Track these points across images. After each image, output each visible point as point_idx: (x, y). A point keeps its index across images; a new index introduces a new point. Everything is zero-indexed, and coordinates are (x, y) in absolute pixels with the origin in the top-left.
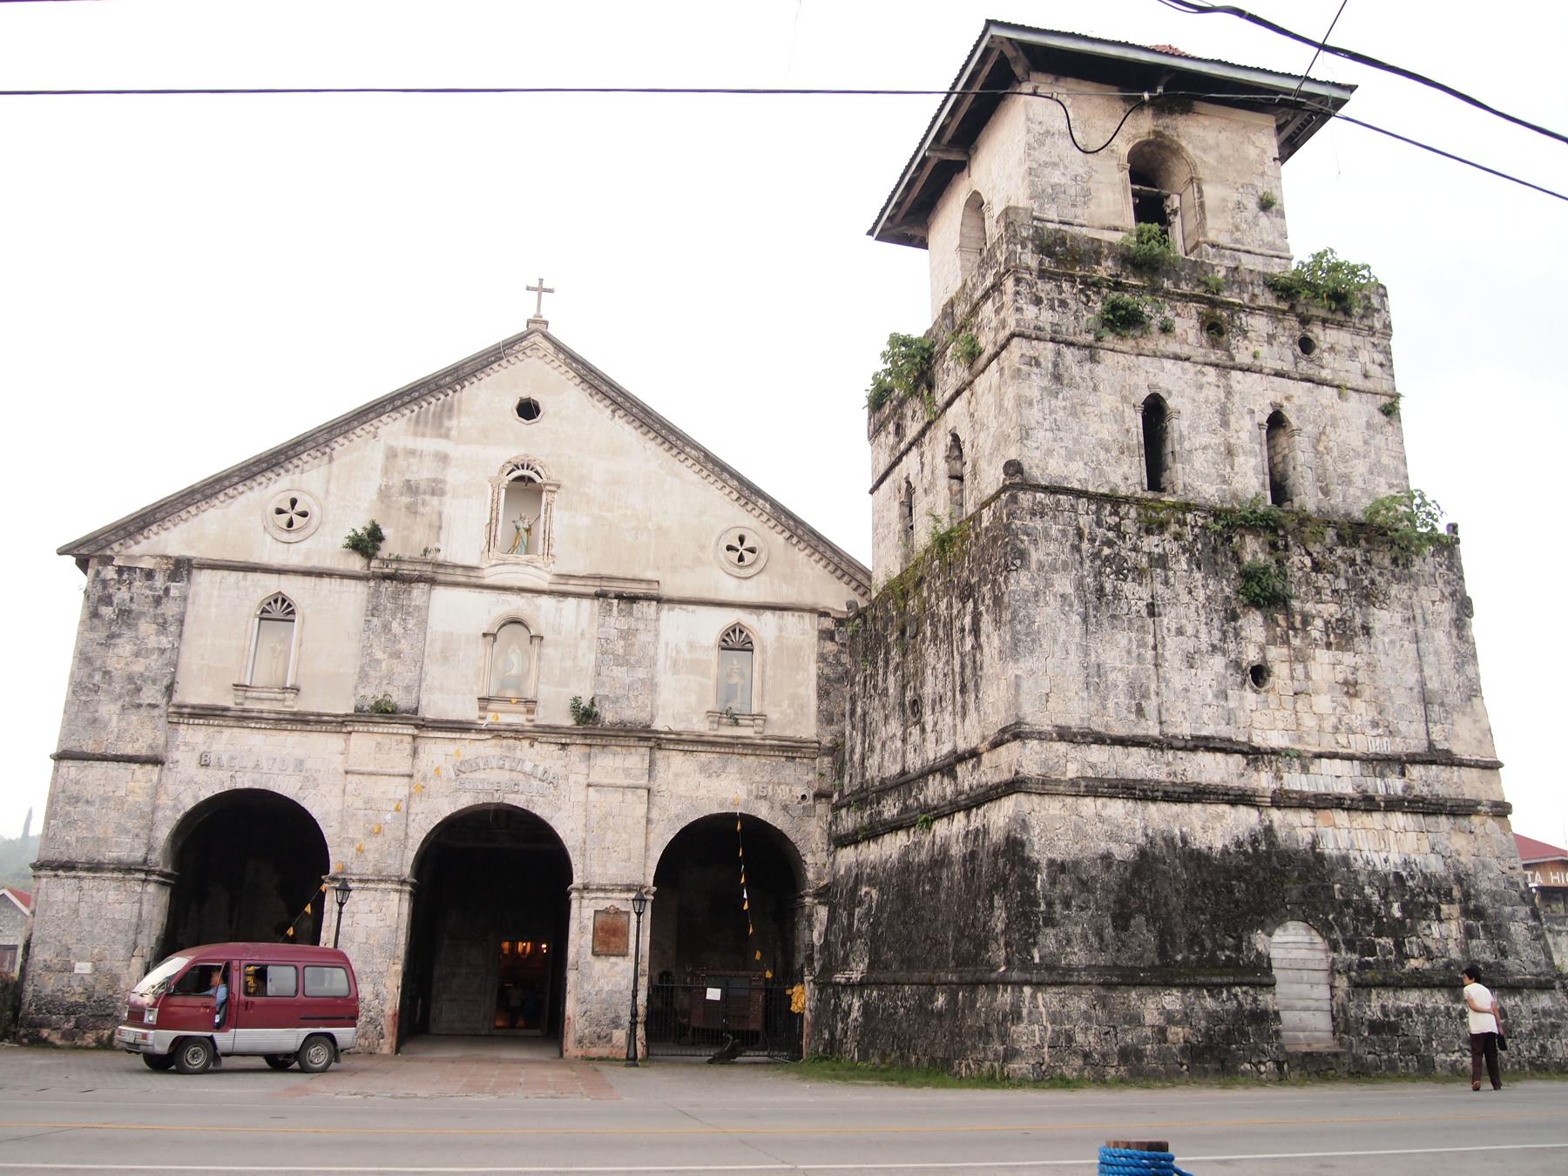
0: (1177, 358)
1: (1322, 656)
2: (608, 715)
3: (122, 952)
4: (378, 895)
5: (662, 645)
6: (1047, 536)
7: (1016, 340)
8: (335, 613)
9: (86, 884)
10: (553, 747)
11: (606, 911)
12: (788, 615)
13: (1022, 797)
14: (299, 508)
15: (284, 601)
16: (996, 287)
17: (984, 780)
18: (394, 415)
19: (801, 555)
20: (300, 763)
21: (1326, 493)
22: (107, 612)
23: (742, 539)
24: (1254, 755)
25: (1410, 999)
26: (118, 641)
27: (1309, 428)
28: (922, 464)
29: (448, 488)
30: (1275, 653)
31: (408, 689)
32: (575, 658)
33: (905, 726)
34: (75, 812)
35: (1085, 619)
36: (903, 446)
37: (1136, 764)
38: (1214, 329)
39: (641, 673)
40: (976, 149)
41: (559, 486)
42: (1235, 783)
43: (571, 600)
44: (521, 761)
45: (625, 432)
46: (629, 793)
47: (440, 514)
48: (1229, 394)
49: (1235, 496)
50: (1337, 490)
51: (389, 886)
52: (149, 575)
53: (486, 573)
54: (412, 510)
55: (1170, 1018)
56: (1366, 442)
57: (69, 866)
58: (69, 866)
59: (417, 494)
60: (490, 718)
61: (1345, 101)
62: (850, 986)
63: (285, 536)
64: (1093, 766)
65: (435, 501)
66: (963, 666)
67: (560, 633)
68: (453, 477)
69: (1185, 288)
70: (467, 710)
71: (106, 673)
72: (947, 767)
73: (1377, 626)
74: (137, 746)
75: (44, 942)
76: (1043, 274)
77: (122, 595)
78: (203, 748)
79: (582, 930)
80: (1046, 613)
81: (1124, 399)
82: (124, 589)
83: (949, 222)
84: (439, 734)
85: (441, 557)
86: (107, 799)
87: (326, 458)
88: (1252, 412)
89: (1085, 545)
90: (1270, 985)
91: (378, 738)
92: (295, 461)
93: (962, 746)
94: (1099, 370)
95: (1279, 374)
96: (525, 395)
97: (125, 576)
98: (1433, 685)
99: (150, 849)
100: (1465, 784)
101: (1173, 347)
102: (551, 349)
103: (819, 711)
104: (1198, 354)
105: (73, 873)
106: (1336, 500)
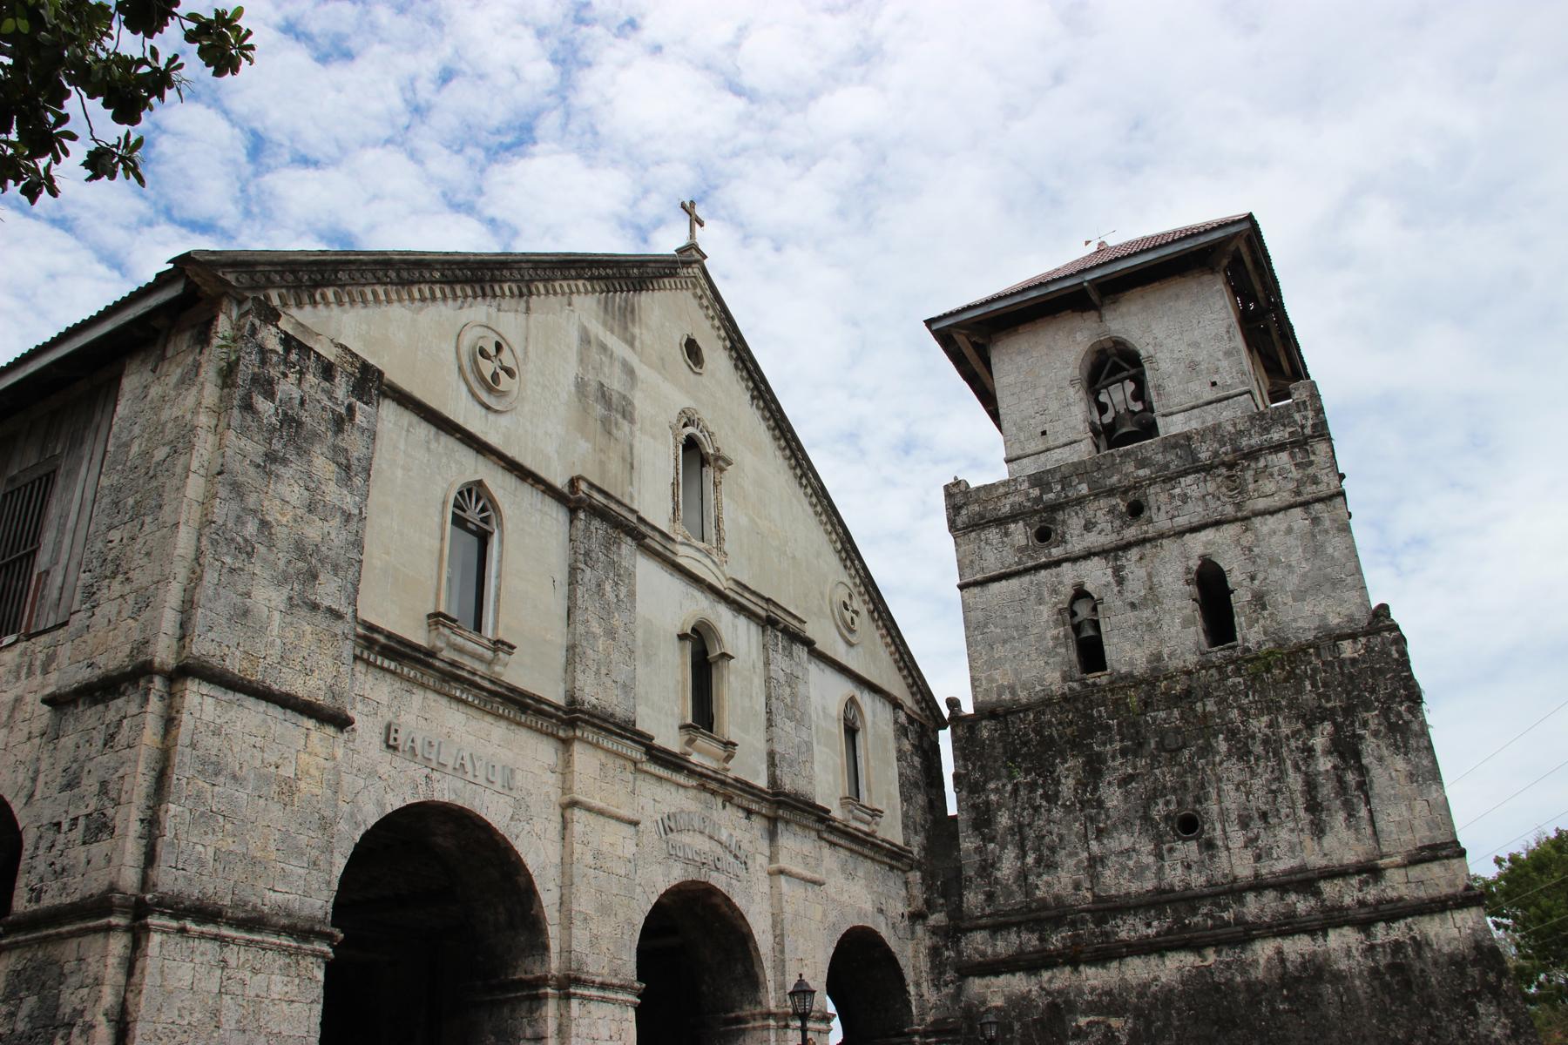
8: (532, 538)
9: (232, 955)
10: (741, 814)
12: (877, 697)
17: (1394, 895)
22: (263, 405)
26: (282, 470)
28: (1120, 581)
33: (1158, 840)
34: (218, 794)
36: (1056, 552)
39: (805, 736)
43: (742, 621)
46: (809, 887)
47: (631, 447)
52: (328, 371)
57: (206, 913)
59: (607, 408)
63: (485, 397)
65: (625, 425)
66: (1311, 786)
68: (642, 404)
71: (264, 524)
72: (1305, 881)
74: (313, 682)
77: (287, 387)
78: (389, 717)
82: (292, 378)
86: (265, 779)
91: (601, 755)
93: (1315, 860)
97: (293, 357)
103: (905, 815)
105: (210, 929)
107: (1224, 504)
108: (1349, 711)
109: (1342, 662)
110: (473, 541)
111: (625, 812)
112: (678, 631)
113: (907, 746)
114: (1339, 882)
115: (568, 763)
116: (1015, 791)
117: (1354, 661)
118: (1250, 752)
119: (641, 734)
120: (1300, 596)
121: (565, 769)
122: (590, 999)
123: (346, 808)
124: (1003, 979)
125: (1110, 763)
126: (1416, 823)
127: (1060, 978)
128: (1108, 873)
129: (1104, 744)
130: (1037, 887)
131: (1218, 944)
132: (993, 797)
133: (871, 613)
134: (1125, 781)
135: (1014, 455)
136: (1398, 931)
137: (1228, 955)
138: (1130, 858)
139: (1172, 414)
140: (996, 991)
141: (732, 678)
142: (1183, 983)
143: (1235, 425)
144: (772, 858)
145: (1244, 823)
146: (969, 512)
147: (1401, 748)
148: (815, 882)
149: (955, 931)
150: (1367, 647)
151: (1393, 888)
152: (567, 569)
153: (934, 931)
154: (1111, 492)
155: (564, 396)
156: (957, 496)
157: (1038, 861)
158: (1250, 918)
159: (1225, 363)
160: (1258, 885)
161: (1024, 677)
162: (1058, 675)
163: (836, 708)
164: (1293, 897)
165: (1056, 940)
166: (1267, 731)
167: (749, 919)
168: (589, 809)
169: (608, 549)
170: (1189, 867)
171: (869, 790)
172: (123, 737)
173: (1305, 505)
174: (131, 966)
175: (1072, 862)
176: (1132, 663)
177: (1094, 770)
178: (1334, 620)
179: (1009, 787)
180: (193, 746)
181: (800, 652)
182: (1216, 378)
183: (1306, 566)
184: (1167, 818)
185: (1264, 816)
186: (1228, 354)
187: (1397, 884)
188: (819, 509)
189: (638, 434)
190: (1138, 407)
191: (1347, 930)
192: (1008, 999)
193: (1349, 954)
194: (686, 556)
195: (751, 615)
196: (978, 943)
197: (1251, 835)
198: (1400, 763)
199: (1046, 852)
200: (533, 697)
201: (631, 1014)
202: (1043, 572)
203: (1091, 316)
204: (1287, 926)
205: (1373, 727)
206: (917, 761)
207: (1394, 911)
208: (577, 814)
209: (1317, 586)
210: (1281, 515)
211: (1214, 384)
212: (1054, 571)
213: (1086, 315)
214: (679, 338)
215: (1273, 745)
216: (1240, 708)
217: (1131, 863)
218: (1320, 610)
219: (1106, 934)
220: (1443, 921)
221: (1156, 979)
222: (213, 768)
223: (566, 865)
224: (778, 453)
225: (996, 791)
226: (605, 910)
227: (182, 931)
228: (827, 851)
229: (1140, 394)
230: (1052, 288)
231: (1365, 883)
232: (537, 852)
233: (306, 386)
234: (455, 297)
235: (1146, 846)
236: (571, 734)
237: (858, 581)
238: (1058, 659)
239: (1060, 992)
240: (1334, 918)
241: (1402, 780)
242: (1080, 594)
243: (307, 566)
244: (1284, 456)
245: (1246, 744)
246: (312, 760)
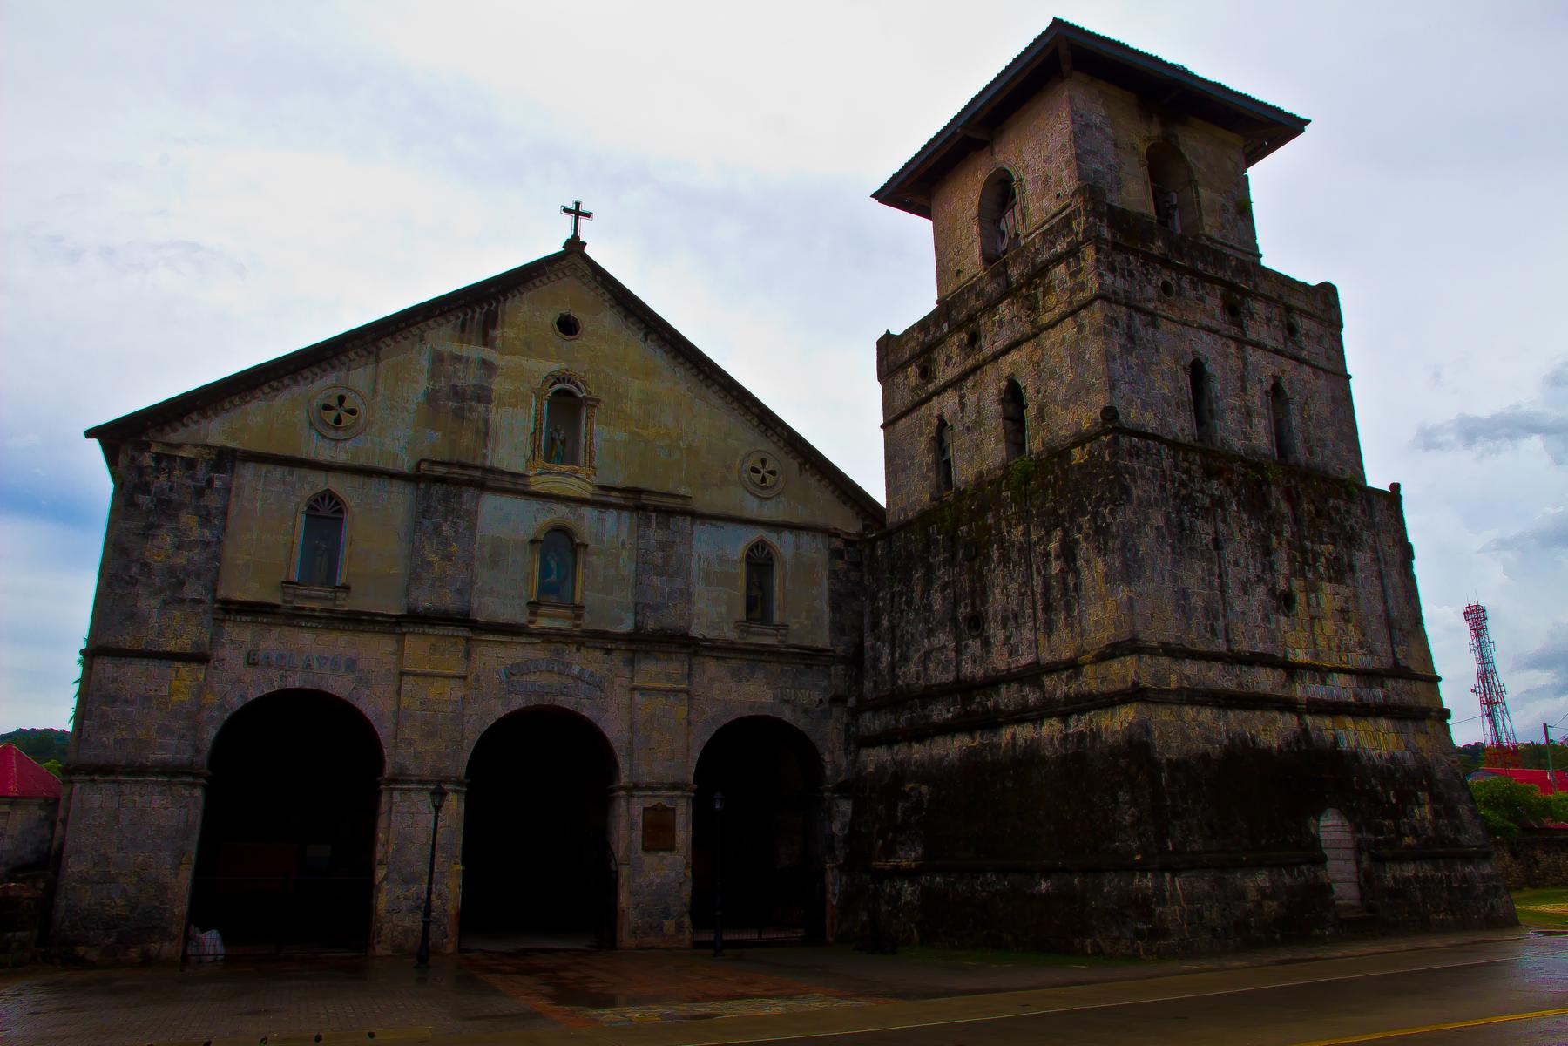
0: (1210, 330)
1: (1327, 587)
5: (695, 556)
6: (1143, 476)
10: (598, 652)
11: (654, 808)
14: (348, 405)
15: (331, 499)
16: (1073, 252)
17: (1085, 689)
18: (441, 320)
20: (352, 665)
21: (1311, 453)
22: (144, 500)
23: (764, 462)
24: (1292, 670)
25: (1409, 870)
27: (1297, 398)
28: (963, 406)
30: (1297, 583)
31: (460, 592)
33: (958, 639)
35: (1173, 551)
36: (930, 388)
37: (1217, 677)
38: (1233, 310)
41: (598, 401)
42: (1280, 693)
44: (569, 665)
45: (658, 358)
47: (487, 421)
48: (1244, 359)
49: (1254, 451)
50: (1317, 450)
52: (190, 464)
54: (459, 415)
55: (1261, 891)
56: (1332, 413)
57: (107, 770)
58: (107, 770)
60: (543, 623)
62: (898, 873)
63: (332, 434)
64: (1188, 678)
65: (481, 408)
66: (1047, 587)
67: (602, 542)
68: (498, 385)
69: (1211, 272)
70: (514, 613)
71: (145, 565)
72: (1034, 674)
73: (1357, 563)
76: (1115, 246)
78: (250, 647)
80: (1146, 543)
81: (1177, 362)
83: (966, 196)
84: (491, 637)
85: (489, 463)
87: (373, 358)
88: (1260, 381)
89: (1168, 486)
90: (1321, 860)
91: (434, 641)
92: (343, 359)
93: (1046, 657)
94: (1158, 335)
95: (1276, 351)
96: (565, 312)
97: (164, 464)
98: (1395, 614)
99: (198, 750)
101: (1206, 321)
102: (589, 271)
104: (1223, 328)
106: (1317, 460)
108: (1072, 516)
112: (531, 533)
114: (1054, 676)
117: (1080, 466)
120: (1065, 408)
121: (400, 653)
122: (410, 790)
124: (874, 751)
127: (901, 751)
136: (1078, 724)
140: (875, 757)
141: (594, 559)
146: (894, 356)
147: (1102, 551)
150: (1090, 453)
156: (887, 344)
157: (901, 655)
160: (1009, 677)
170: (974, 661)
177: (928, 581)
178: (1085, 426)
181: (684, 523)
187: (1091, 681)
191: (1054, 721)
194: (538, 483)
204: (1022, 715)
205: (1085, 531)
208: (405, 678)
214: (550, 318)
215: (1026, 550)
216: (1007, 519)
220: (1113, 715)
225: (883, 599)
227: (93, 781)
232: (374, 704)
242: (942, 424)
243: (177, 577)
244: (1062, 267)
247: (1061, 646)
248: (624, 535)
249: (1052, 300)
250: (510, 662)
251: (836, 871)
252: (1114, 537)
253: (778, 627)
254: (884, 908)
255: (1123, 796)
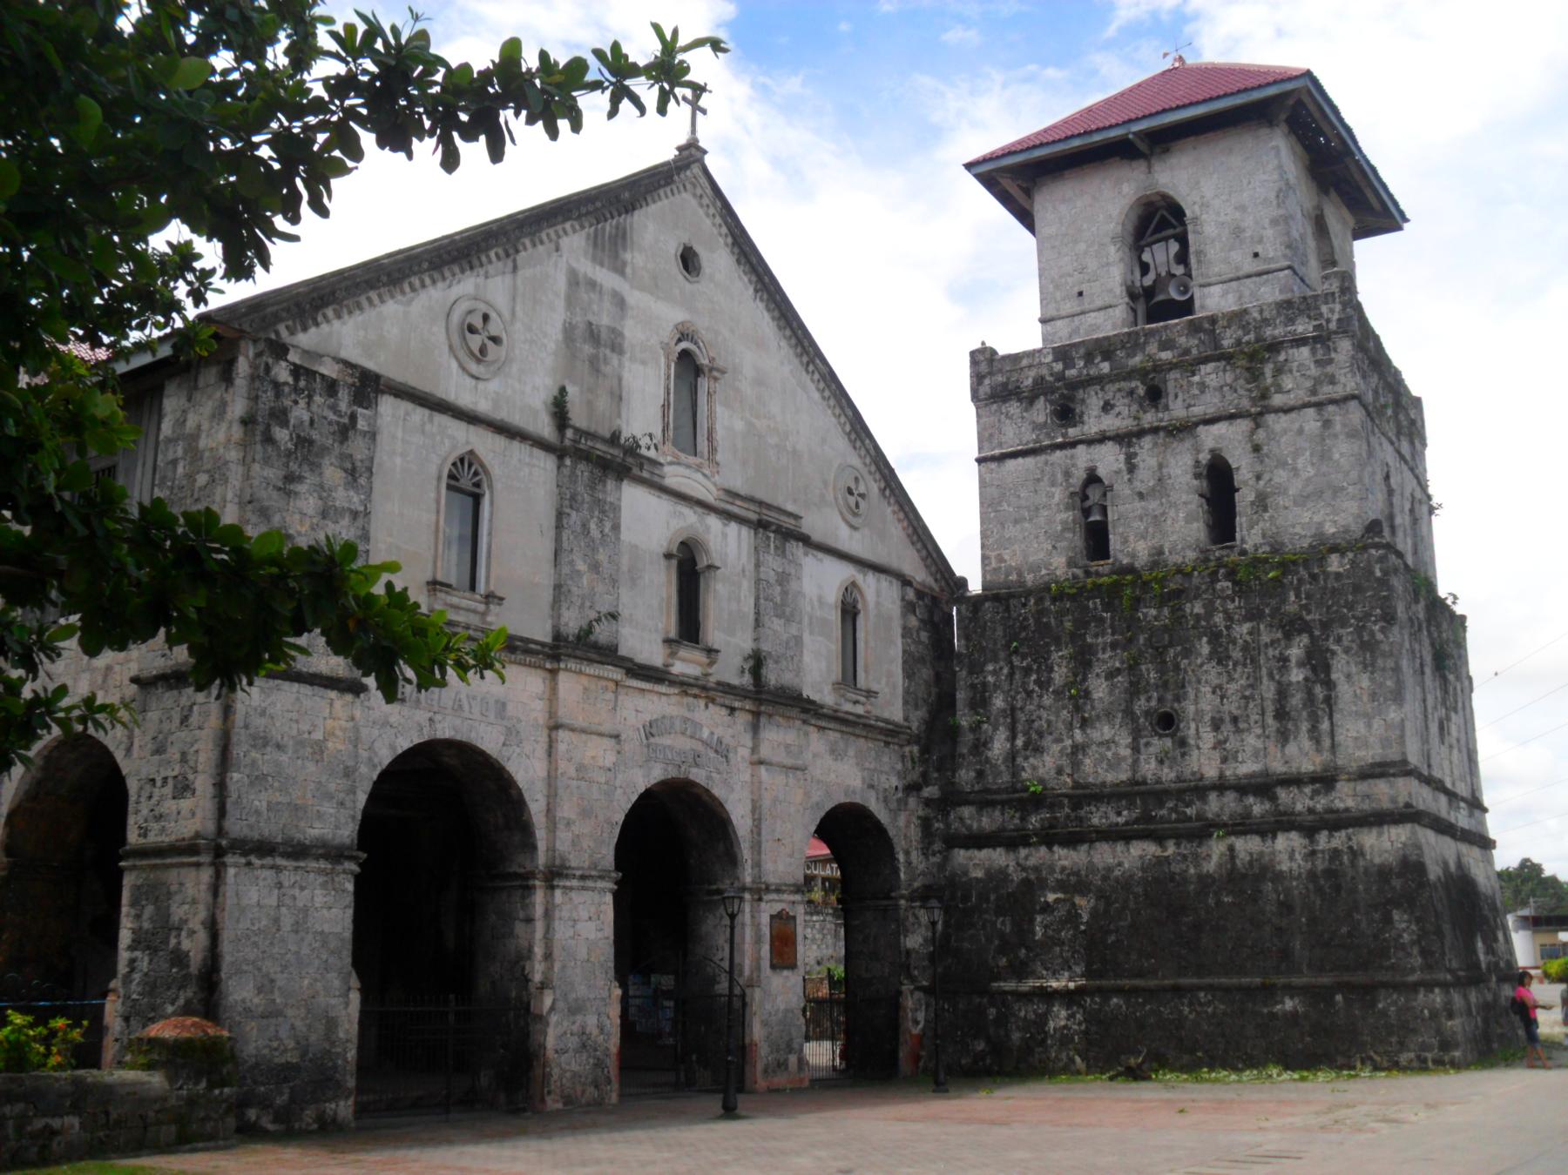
2: (772, 676)
3: (337, 983)
4: (596, 896)
7: (1353, 404)
9: (288, 878)
10: (724, 712)
12: (883, 577)
13: (1417, 827)
14: (495, 328)
17: (1341, 806)
19: (889, 511)
20: (502, 706)
28: (1132, 468)
29: (626, 345)
32: (739, 601)
33: (1136, 734)
34: (265, 760)
39: (794, 630)
40: (1167, 151)
45: (765, 323)
47: (620, 379)
51: (600, 884)
52: (331, 387)
53: (667, 469)
54: (595, 364)
57: (264, 848)
58: (264, 848)
59: (594, 344)
60: (678, 668)
61: (1400, 228)
62: (1048, 996)
63: (473, 367)
65: (614, 359)
66: (1282, 693)
68: (632, 332)
72: (1264, 786)
75: (239, 972)
77: (299, 413)
79: (758, 940)
82: (302, 403)
86: (301, 744)
91: (584, 681)
93: (1278, 767)
97: (302, 384)
100: (1462, 819)
102: (709, 191)
103: (907, 692)
105: (268, 861)
107: (1241, 397)
108: (1325, 626)
109: (1327, 575)
110: (470, 500)
111: (607, 728)
112: (663, 550)
113: (913, 622)
115: (554, 690)
116: (1011, 675)
117: (1338, 576)
118: (1229, 657)
119: (624, 659)
120: (1302, 500)
122: (571, 889)
123: (364, 754)
124: (984, 854)
125: (1100, 656)
126: (1372, 739)
127: (1037, 856)
128: (1087, 761)
129: (1096, 636)
130: (1023, 769)
131: (1178, 837)
132: (990, 679)
133: (883, 491)
134: (1110, 675)
135: (1052, 313)
136: (1339, 840)
137: (1186, 848)
138: (1109, 749)
139: (1209, 285)
140: (977, 862)
141: (719, 586)
142: (1143, 869)
143: (1261, 312)
144: (754, 750)
145: (1216, 725)
146: (995, 381)
148: (795, 768)
149: (951, 799)
150: (1353, 562)
151: (1341, 800)
152: (554, 513)
153: (928, 803)
154: (1130, 375)
155: (552, 346)
156: (984, 362)
157: (1026, 746)
158: (1210, 816)
159: (1269, 233)
160: (1221, 786)
161: (1031, 559)
162: (1063, 560)
163: (833, 596)
164: (1251, 800)
165: (1034, 821)
166: (1248, 638)
167: (728, 807)
168: (573, 730)
169: (593, 488)
171: (866, 672)
172: (194, 719)
173: (1319, 405)
174: (216, 889)
175: (1056, 748)
176: (1133, 556)
177: (1083, 661)
178: (1330, 529)
179: (1005, 671)
180: (246, 727)
181: (796, 549)
182: (1259, 249)
183: (1311, 471)
184: (1147, 713)
185: (1235, 720)
186: (1274, 222)
187: (1345, 797)
188: (827, 393)
189: (627, 364)
190: (1179, 270)
191: (1294, 835)
192: (988, 872)
193: (1292, 858)
194: (674, 477)
195: (742, 521)
196: (969, 817)
197: (1221, 737)
198: (1365, 681)
199: (1034, 736)
200: (522, 639)
201: (609, 898)
202: (1058, 453)
203: (1141, 165)
204: (1242, 826)
205: (1345, 643)
206: (924, 636)
207: (1337, 821)
208: (562, 734)
209: (1319, 494)
210: (1293, 415)
211: (1256, 255)
212: (1068, 452)
213: (1135, 164)
214: (673, 248)
216: (1226, 612)
217: (1109, 754)
218: (1316, 519)
219: (1080, 819)
220: (1380, 835)
221: (1120, 864)
222: (262, 741)
223: (551, 780)
224: (783, 343)
225: (994, 673)
226: (586, 813)
227: (249, 864)
228: (814, 735)
229: (1182, 258)
230: (1097, 138)
231: (1315, 793)
232: (527, 771)
233: (314, 408)
234: (444, 279)
235: (1125, 739)
236: (555, 666)
237: (868, 460)
238: (1065, 544)
239: (1036, 869)
240: (1282, 822)
241: (1365, 698)
242: (1093, 478)
245: (1227, 649)
246: (336, 724)
247: (1302, 756)
248: (744, 559)
249: (1287, 382)
250: (648, 718)
251: (918, 995)
252: (1384, 655)
253: (870, 694)
254: (1016, 1036)
255: (1396, 915)
